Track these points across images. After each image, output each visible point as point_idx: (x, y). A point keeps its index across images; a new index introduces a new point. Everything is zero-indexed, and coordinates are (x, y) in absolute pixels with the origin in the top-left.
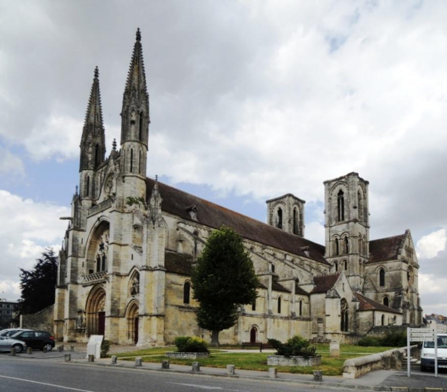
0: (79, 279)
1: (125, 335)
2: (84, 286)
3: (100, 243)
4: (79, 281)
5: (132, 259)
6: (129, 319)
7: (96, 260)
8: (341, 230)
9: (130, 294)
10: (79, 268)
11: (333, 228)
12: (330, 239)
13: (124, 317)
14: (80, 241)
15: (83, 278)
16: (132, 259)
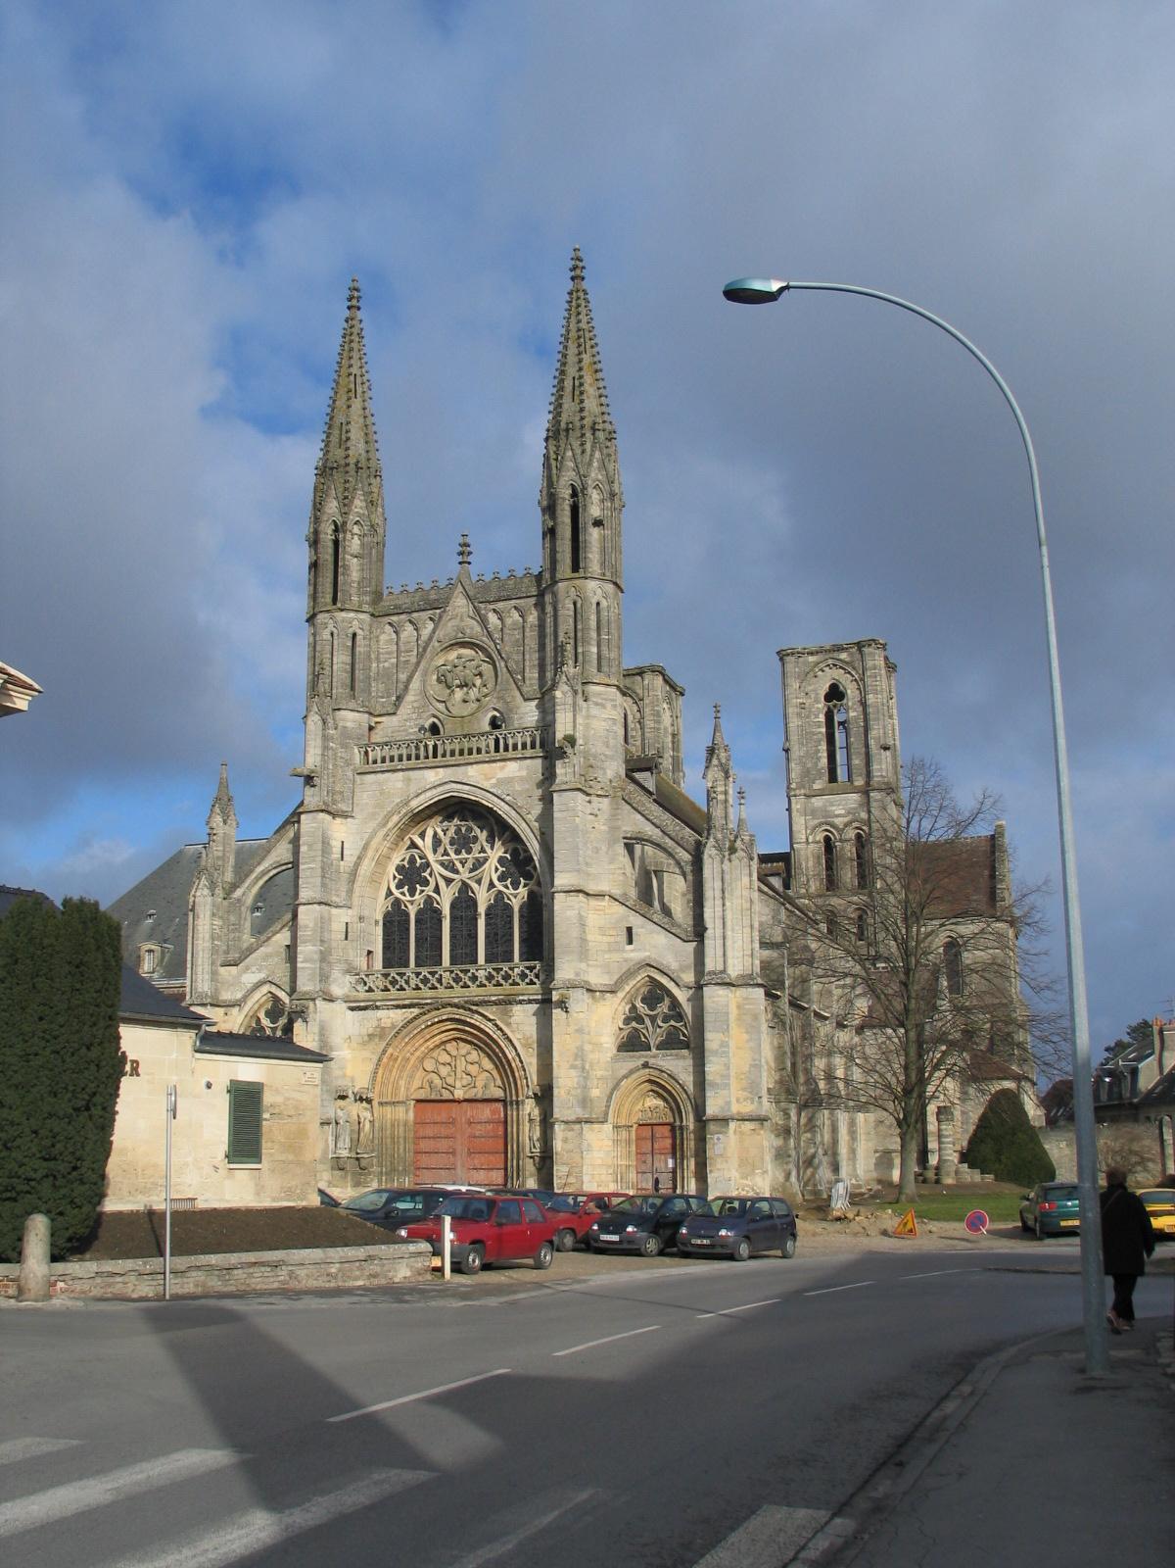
0: (335, 980)
1: (610, 1178)
2: (352, 1009)
3: (399, 857)
4: (337, 990)
5: (630, 942)
6: (616, 1127)
7: (380, 917)
8: (843, 812)
9: (615, 1051)
10: (334, 944)
11: (817, 802)
12: (807, 840)
13: (604, 1121)
14: (337, 850)
15: (349, 979)
16: (630, 942)
